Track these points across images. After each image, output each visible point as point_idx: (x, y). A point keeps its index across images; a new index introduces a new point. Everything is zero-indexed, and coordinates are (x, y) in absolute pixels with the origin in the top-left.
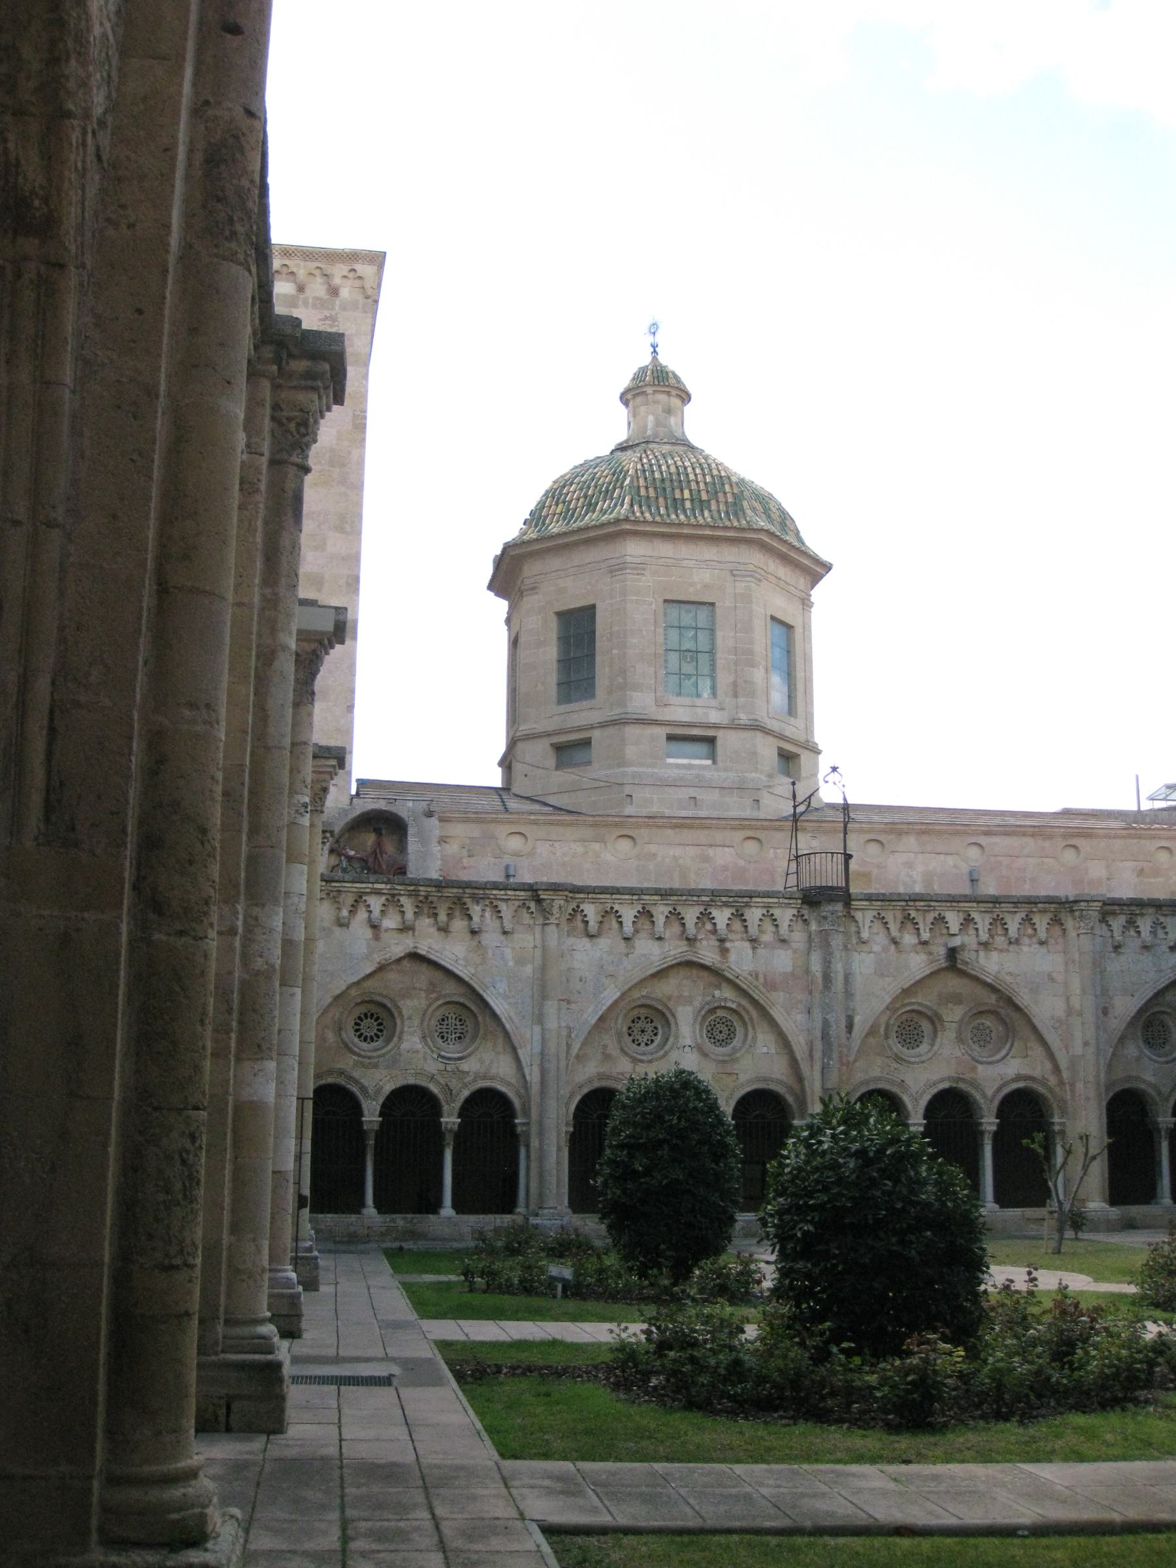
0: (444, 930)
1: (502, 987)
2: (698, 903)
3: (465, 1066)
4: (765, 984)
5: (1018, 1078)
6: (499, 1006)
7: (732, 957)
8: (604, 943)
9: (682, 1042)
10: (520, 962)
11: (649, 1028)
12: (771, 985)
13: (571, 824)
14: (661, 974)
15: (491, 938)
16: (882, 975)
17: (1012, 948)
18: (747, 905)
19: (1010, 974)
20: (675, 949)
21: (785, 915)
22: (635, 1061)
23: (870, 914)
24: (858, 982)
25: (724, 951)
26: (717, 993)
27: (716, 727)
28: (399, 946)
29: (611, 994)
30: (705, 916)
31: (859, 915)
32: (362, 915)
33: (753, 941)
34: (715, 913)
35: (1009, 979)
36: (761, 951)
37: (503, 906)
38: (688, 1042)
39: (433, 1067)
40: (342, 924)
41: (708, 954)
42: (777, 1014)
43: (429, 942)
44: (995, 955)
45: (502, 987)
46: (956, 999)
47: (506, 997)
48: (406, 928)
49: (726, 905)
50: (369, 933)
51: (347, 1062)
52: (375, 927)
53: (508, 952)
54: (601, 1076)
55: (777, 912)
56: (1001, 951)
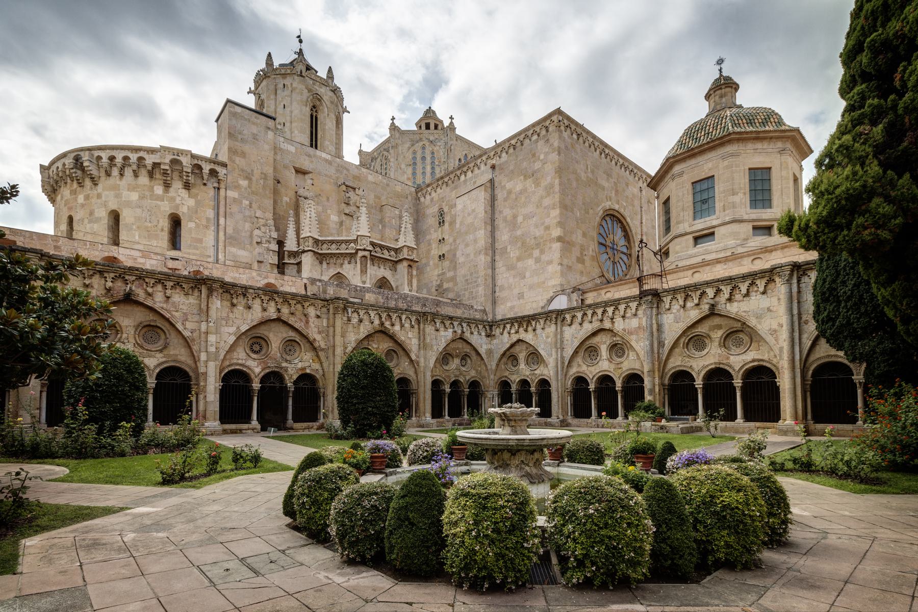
0: (526, 331)
1: (542, 346)
2: (601, 307)
3: (536, 372)
4: (628, 333)
5: (753, 361)
6: (542, 353)
7: (616, 325)
8: (573, 326)
9: (603, 358)
10: (547, 337)
11: (596, 354)
12: (630, 333)
13: (625, 284)
14: (594, 334)
15: (539, 331)
16: (677, 322)
17: (745, 299)
18: (619, 304)
19: (745, 312)
20: (596, 325)
21: (634, 305)
22: (588, 366)
23: (669, 298)
24: (666, 328)
25: (613, 323)
26: (614, 339)
27: (714, 227)
28: (515, 338)
29: (576, 343)
30: (604, 312)
31: (664, 299)
32: (506, 331)
33: (623, 317)
34: (608, 309)
35: (744, 314)
36: (627, 320)
37: (541, 320)
38: (605, 357)
39: (528, 373)
40: (502, 334)
41: (607, 325)
42: (633, 344)
43: (523, 335)
44: (735, 304)
45: (542, 346)
46: (719, 327)
47: (543, 349)
48: (517, 332)
49: (611, 305)
50: (508, 335)
51: (507, 374)
52: (509, 333)
53: (544, 335)
54: (578, 372)
55: (630, 304)
56: (740, 301)
